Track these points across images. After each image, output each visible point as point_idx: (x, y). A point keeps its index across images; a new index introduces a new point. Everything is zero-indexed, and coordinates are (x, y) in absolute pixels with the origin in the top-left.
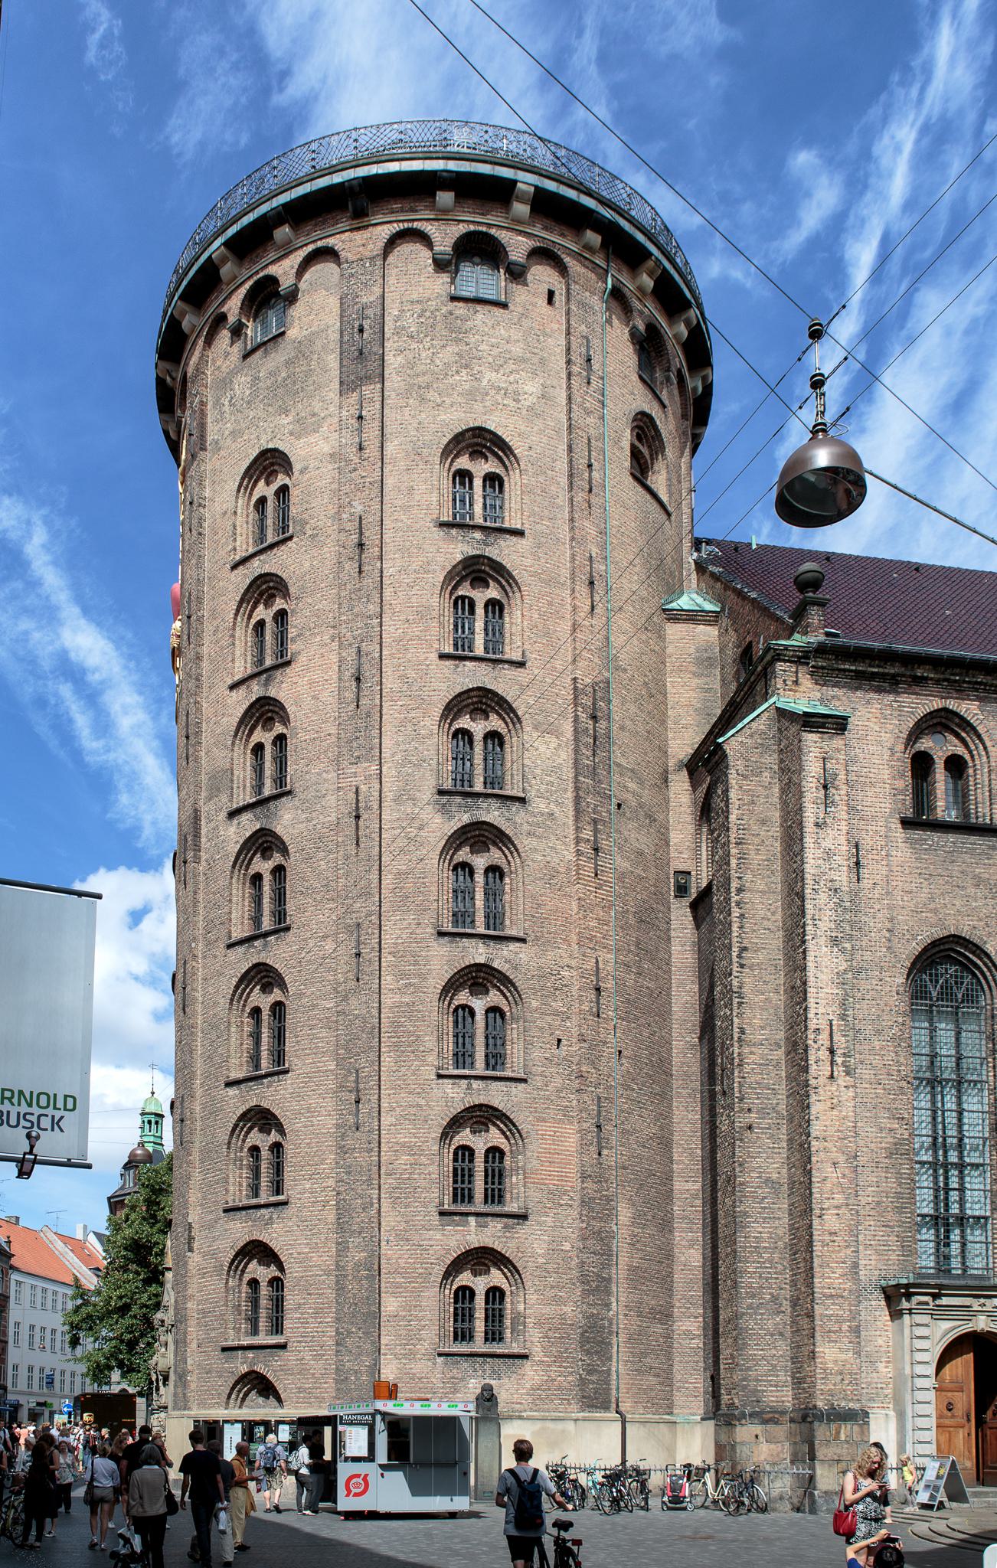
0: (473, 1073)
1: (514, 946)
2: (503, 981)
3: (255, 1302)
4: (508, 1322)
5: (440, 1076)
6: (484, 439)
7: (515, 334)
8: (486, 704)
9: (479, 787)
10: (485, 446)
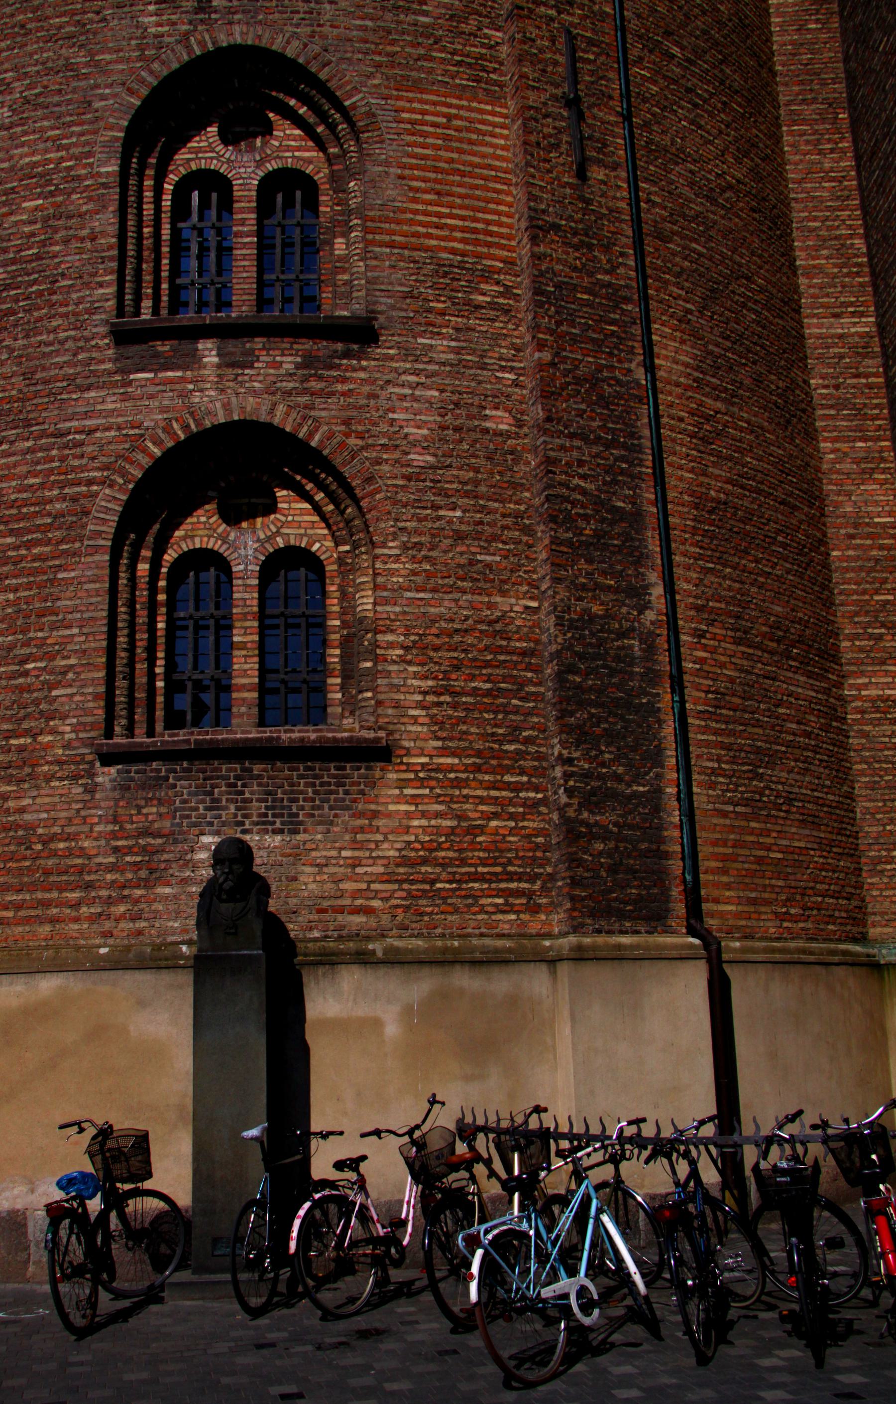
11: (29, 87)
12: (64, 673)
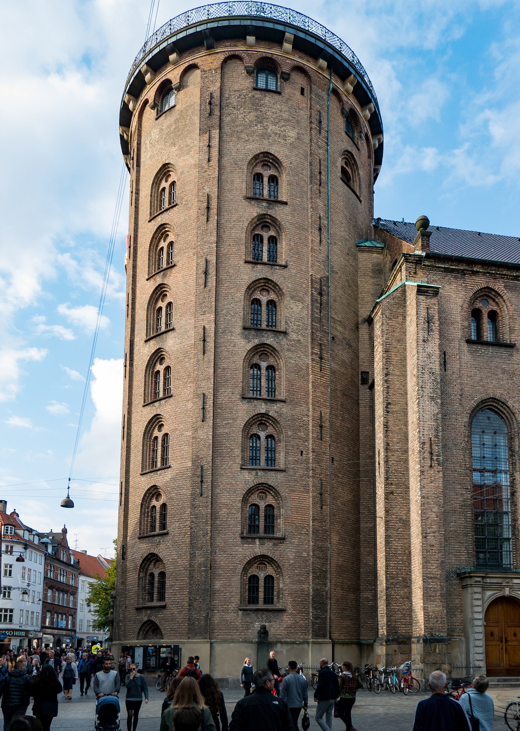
0: (259, 467)
1: (279, 405)
2: (275, 421)
3: (152, 584)
4: (275, 593)
5: (242, 468)
6: (269, 158)
7: (284, 108)
8: (268, 286)
9: (264, 326)
10: (269, 162)
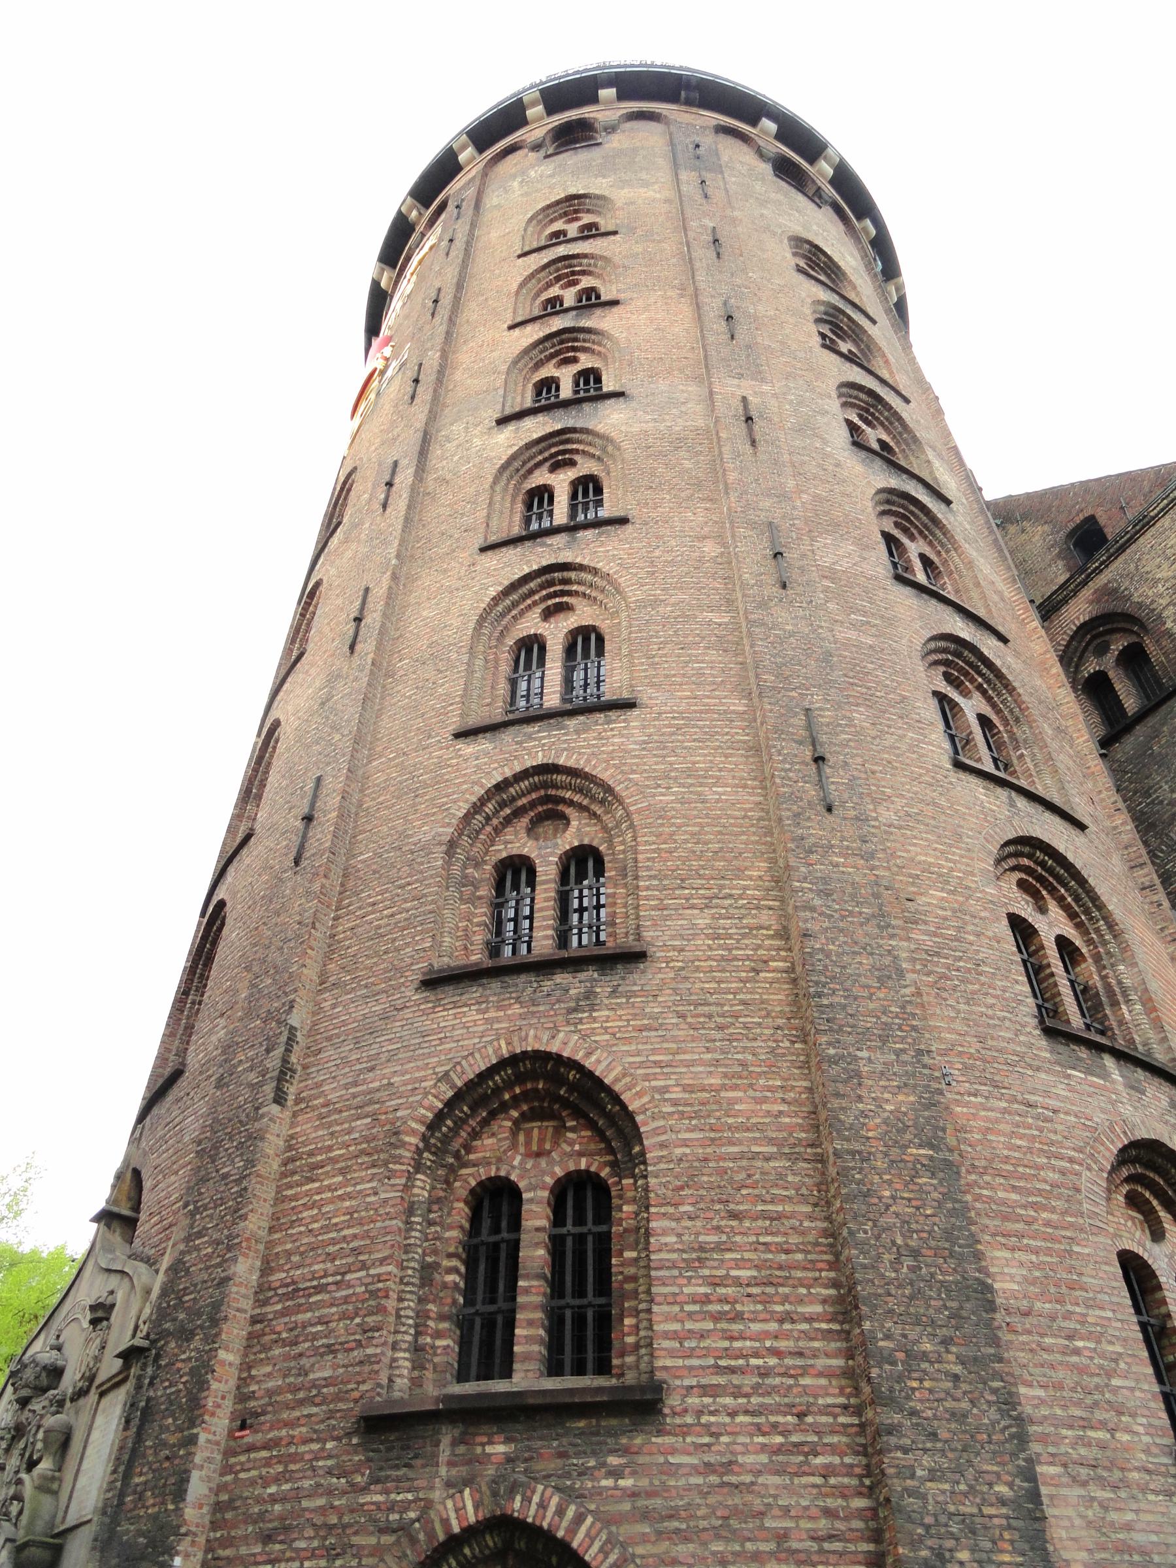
8: (872, 415)
11: (907, 805)
12: (1116, 1361)
